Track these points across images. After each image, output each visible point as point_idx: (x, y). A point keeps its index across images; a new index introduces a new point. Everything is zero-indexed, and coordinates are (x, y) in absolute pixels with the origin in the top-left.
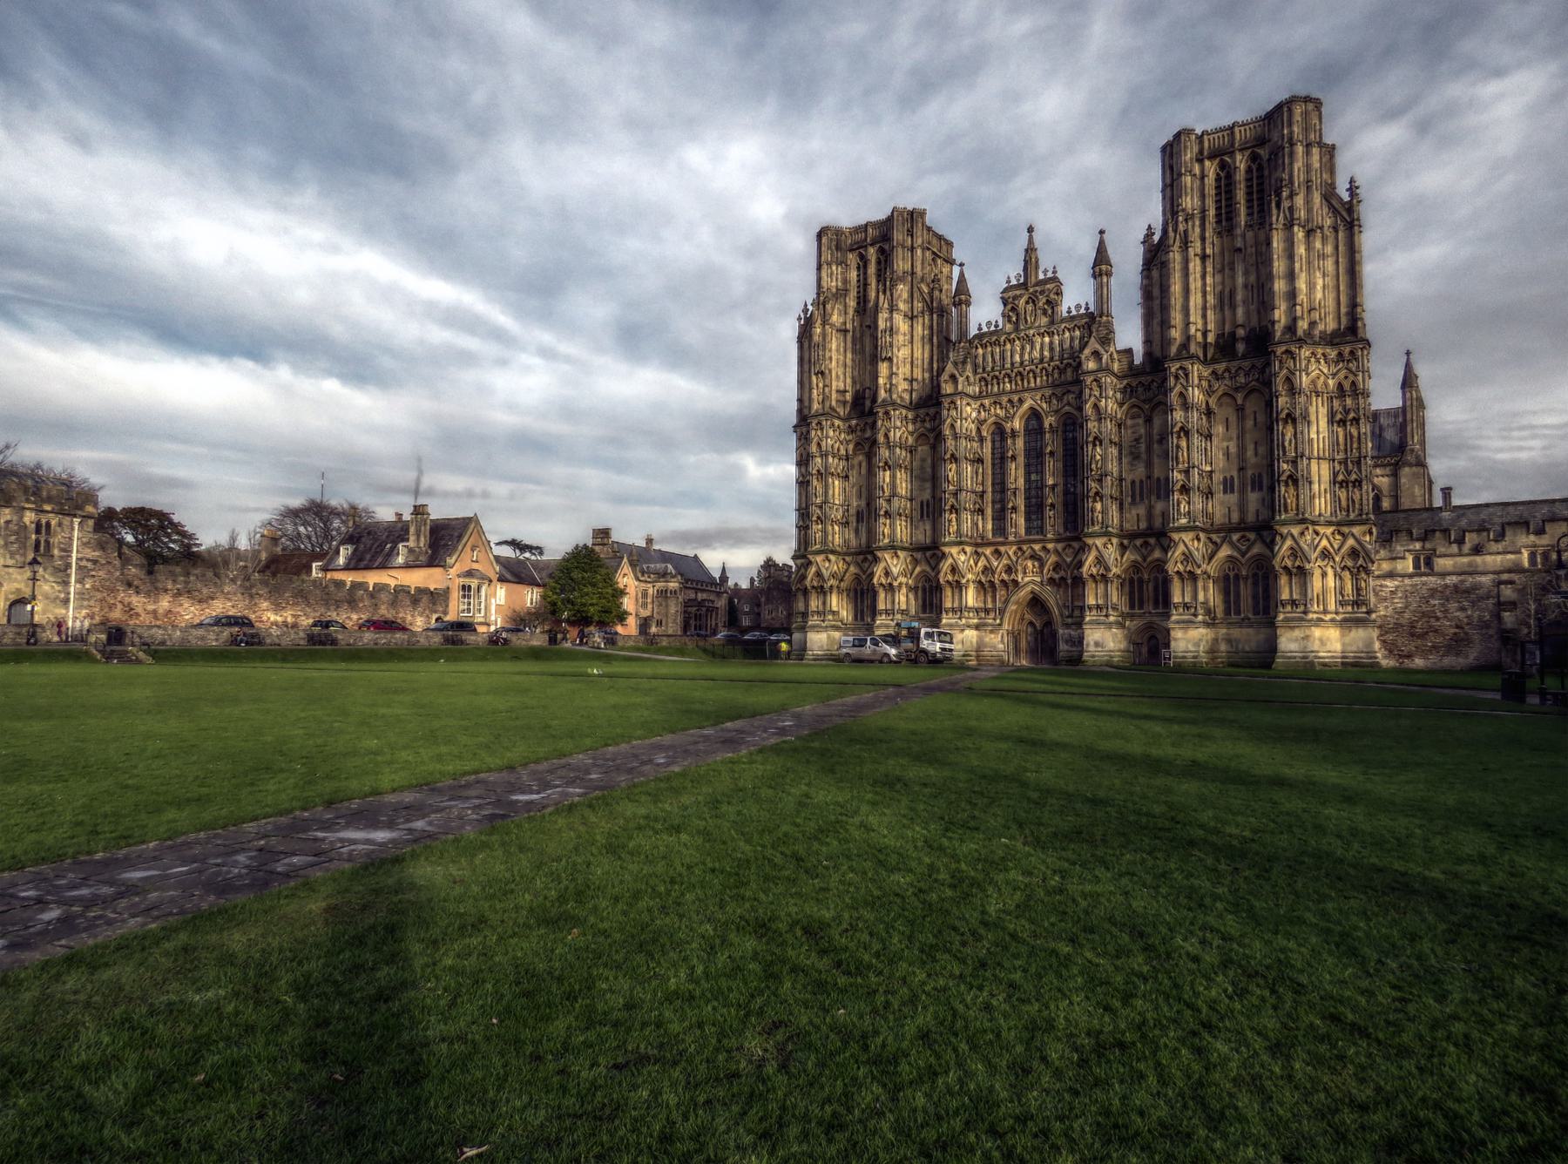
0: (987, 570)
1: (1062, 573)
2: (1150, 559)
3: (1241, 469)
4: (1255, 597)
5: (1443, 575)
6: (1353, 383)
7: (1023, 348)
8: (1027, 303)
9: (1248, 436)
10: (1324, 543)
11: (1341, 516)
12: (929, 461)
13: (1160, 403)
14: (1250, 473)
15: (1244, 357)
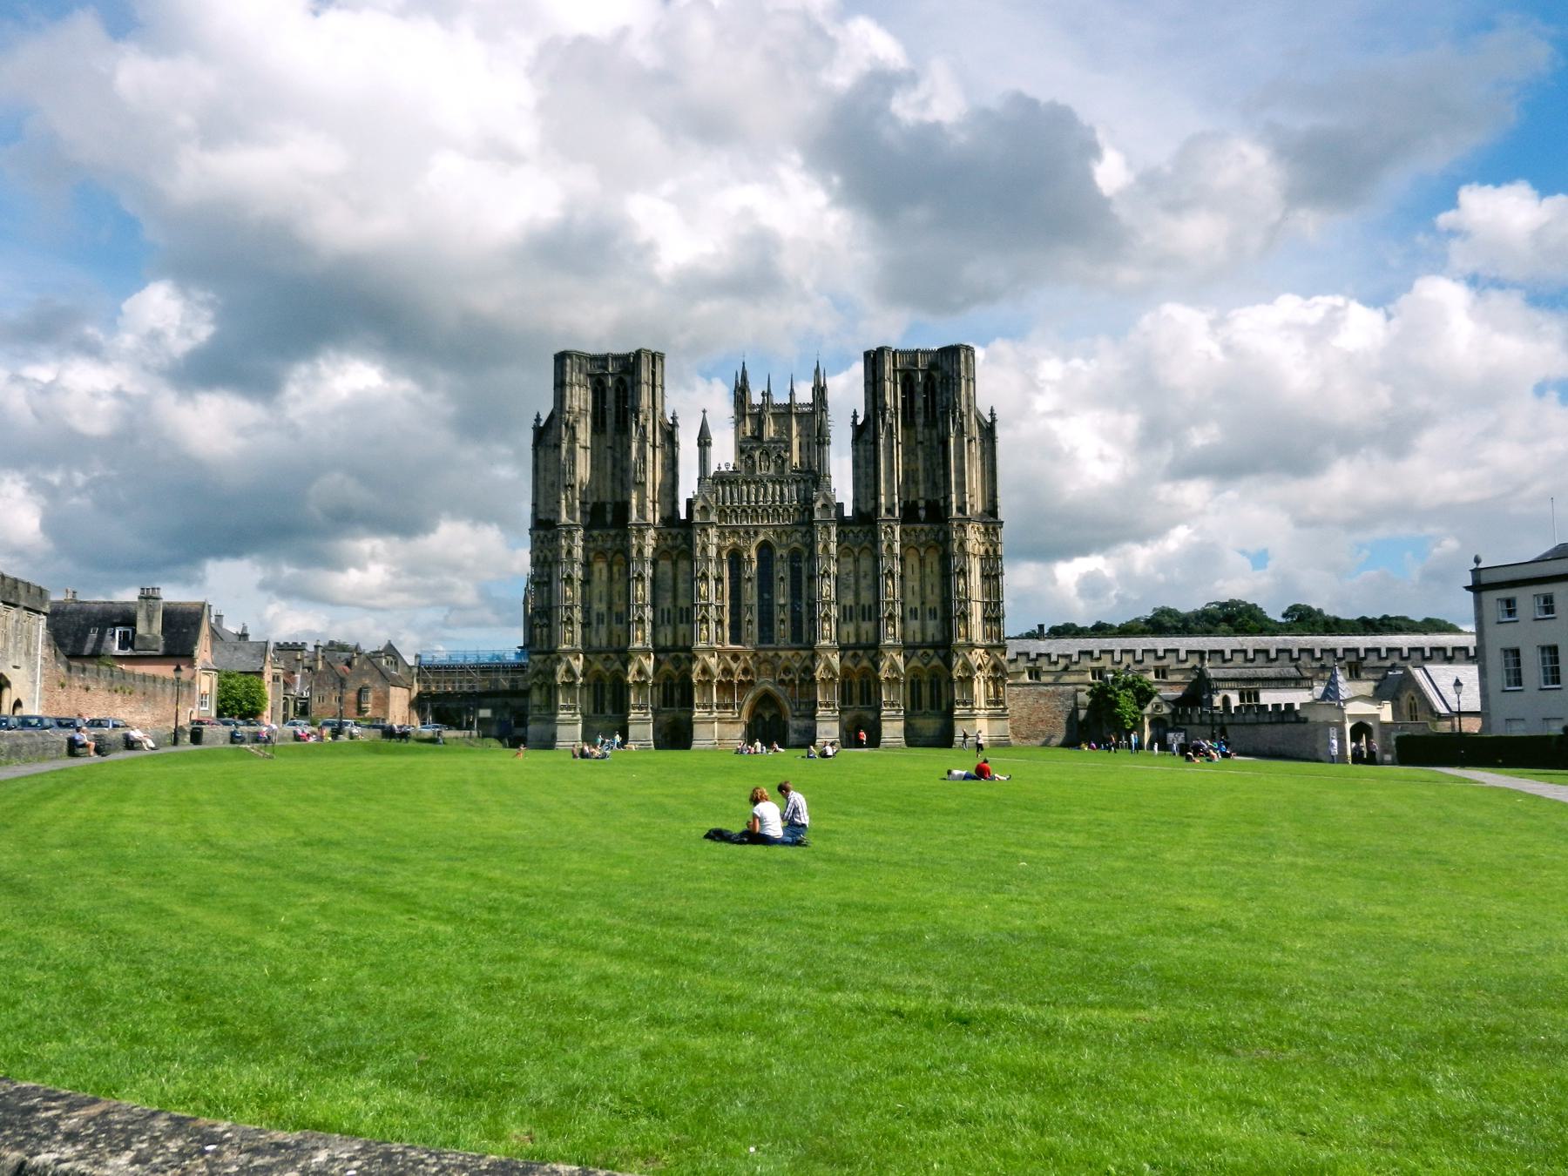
0: (727, 671)
1: (791, 676)
2: (859, 667)
3: (923, 603)
4: (932, 696)
5: (1046, 685)
6: (995, 551)
7: (757, 490)
8: (761, 453)
9: (927, 579)
10: (979, 661)
11: (988, 642)
12: (670, 574)
13: (866, 548)
14: (928, 606)
15: (925, 522)
